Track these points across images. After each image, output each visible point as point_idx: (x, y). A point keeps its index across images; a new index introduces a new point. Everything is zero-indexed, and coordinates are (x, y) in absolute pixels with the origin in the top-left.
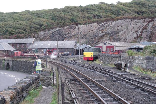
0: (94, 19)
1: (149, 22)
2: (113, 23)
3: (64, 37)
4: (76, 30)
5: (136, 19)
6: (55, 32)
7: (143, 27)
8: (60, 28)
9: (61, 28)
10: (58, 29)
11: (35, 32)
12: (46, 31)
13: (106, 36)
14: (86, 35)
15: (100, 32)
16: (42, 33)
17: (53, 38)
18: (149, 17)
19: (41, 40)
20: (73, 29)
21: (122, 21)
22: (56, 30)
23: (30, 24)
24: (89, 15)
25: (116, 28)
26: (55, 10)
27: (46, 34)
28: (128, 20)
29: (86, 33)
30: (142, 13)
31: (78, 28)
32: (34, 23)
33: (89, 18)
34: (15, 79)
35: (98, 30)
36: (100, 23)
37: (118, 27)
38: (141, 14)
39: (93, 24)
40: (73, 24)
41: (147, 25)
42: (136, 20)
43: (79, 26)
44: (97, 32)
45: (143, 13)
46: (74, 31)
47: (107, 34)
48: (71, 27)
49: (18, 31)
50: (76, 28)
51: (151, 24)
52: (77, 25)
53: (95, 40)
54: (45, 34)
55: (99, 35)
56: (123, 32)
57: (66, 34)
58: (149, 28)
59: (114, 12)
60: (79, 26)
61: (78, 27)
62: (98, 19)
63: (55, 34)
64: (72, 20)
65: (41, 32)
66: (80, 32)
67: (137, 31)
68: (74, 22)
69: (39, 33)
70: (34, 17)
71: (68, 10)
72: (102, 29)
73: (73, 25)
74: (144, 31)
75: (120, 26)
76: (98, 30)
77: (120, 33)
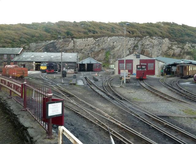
0: (91, 34)
1: (139, 41)
2: (109, 39)
4: (71, 45)
5: (128, 37)
7: (134, 45)
8: (54, 41)
9: (56, 41)
10: (52, 41)
11: (26, 43)
13: (102, 51)
14: (82, 50)
15: (97, 47)
16: (33, 45)
17: (47, 49)
18: (139, 37)
19: (33, 52)
20: (68, 43)
21: (117, 37)
22: (49, 42)
23: (20, 35)
24: (84, 30)
25: (112, 44)
26: (49, 23)
27: (39, 46)
28: (122, 37)
29: (82, 48)
30: (132, 32)
31: (74, 42)
32: (25, 33)
33: (85, 33)
35: (94, 45)
36: (97, 38)
37: (114, 43)
38: (132, 33)
39: (89, 39)
40: (68, 38)
41: (137, 43)
42: (128, 38)
43: (75, 40)
44: (93, 47)
45: (133, 32)
47: (103, 49)
49: (4, 40)
51: (140, 43)
52: (72, 38)
53: (91, 55)
54: (37, 46)
55: (96, 50)
56: (118, 48)
57: (61, 48)
58: (140, 46)
59: (108, 29)
61: (74, 41)
62: (94, 35)
63: (48, 46)
64: (68, 33)
65: (32, 44)
66: (76, 46)
67: (129, 49)
69: (30, 44)
70: (25, 28)
71: (62, 24)
72: (99, 44)
73: (69, 39)
74: (136, 48)
75: (115, 43)
76: (94, 45)
77: (116, 49)
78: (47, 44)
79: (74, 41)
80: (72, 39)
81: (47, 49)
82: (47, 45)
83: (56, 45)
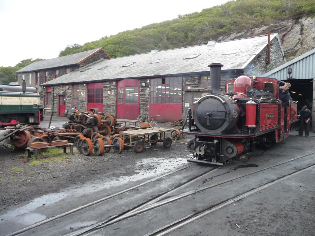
31: (302, 30)
40: (282, 20)
46: (288, 40)
48: (276, 29)
50: (292, 29)
61: (302, 25)
80: (297, 23)
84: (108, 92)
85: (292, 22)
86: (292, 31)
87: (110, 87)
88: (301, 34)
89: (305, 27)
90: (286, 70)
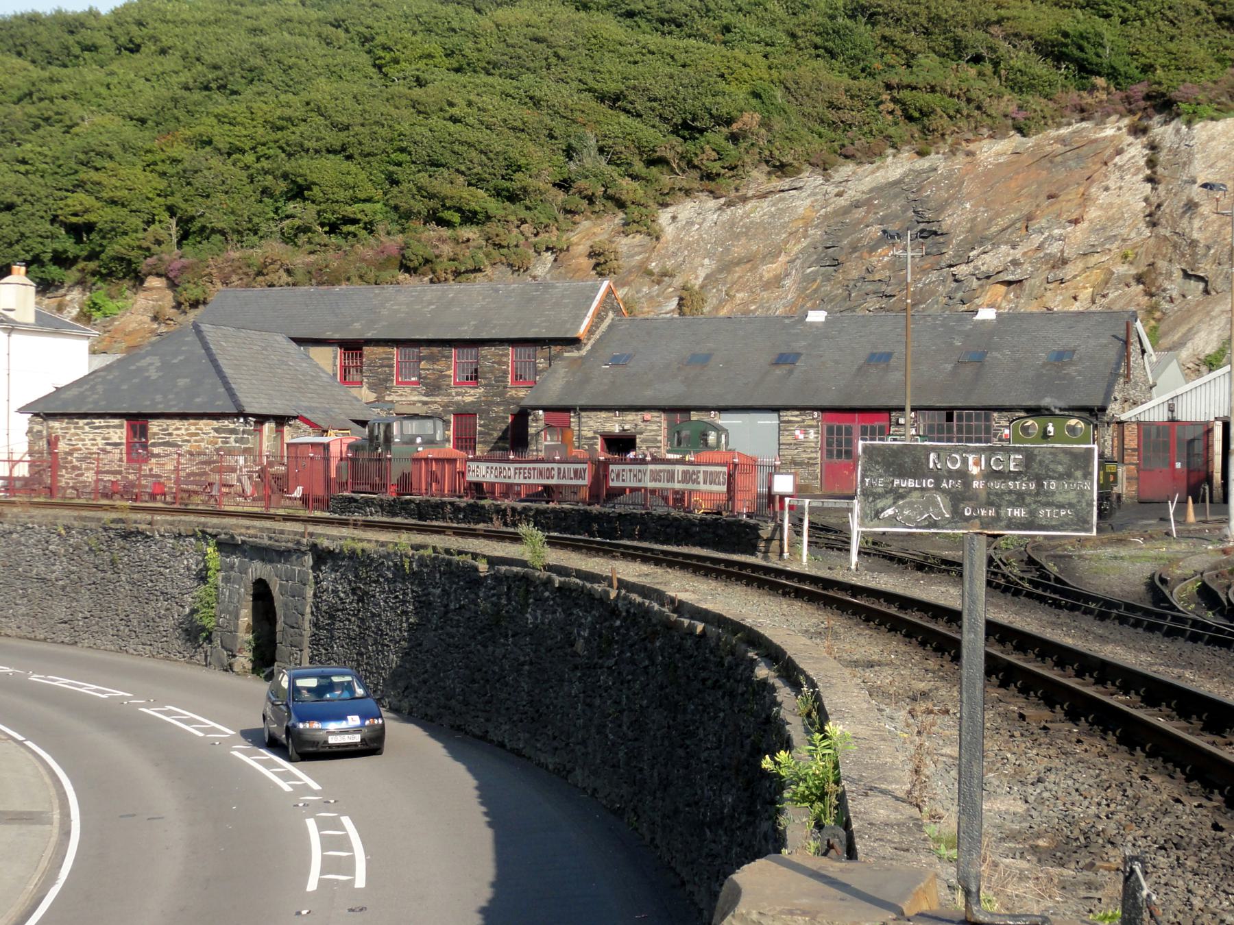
3: (962, 270)
6: (859, 213)
12: (745, 199)
31: (1151, 163)
34: (311, 824)
40: (1084, 113)
50: (1119, 152)
54: (732, 231)
60: (1170, 128)
65: (686, 209)
68: (1100, 81)
69: (664, 217)
78: (842, 201)
79: (1153, 147)
80: (1138, 131)
81: (836, 263)
82: (846, 211)
83: (941, 208)
84: (797, 432)
85: (1119, 129)
86: (1117, 159)
87: (803, 421)
88: (1150, 180)
89: (1162, 156)
90: (1166, 405)
